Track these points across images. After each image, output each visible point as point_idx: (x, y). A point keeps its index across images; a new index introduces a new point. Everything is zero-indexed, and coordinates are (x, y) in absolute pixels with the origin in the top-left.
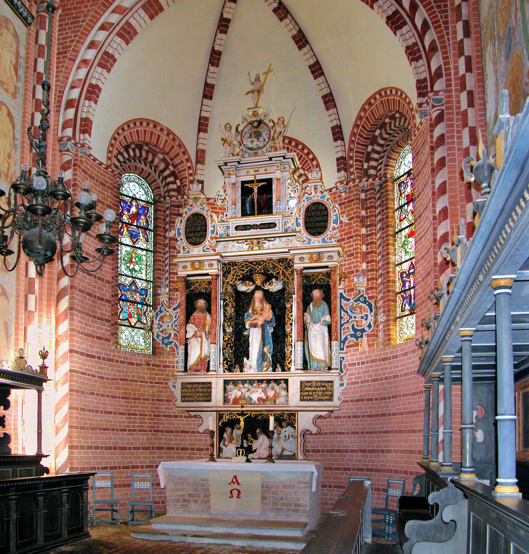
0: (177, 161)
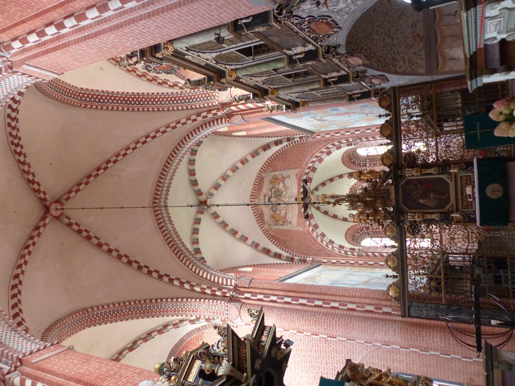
0: (357, 229)
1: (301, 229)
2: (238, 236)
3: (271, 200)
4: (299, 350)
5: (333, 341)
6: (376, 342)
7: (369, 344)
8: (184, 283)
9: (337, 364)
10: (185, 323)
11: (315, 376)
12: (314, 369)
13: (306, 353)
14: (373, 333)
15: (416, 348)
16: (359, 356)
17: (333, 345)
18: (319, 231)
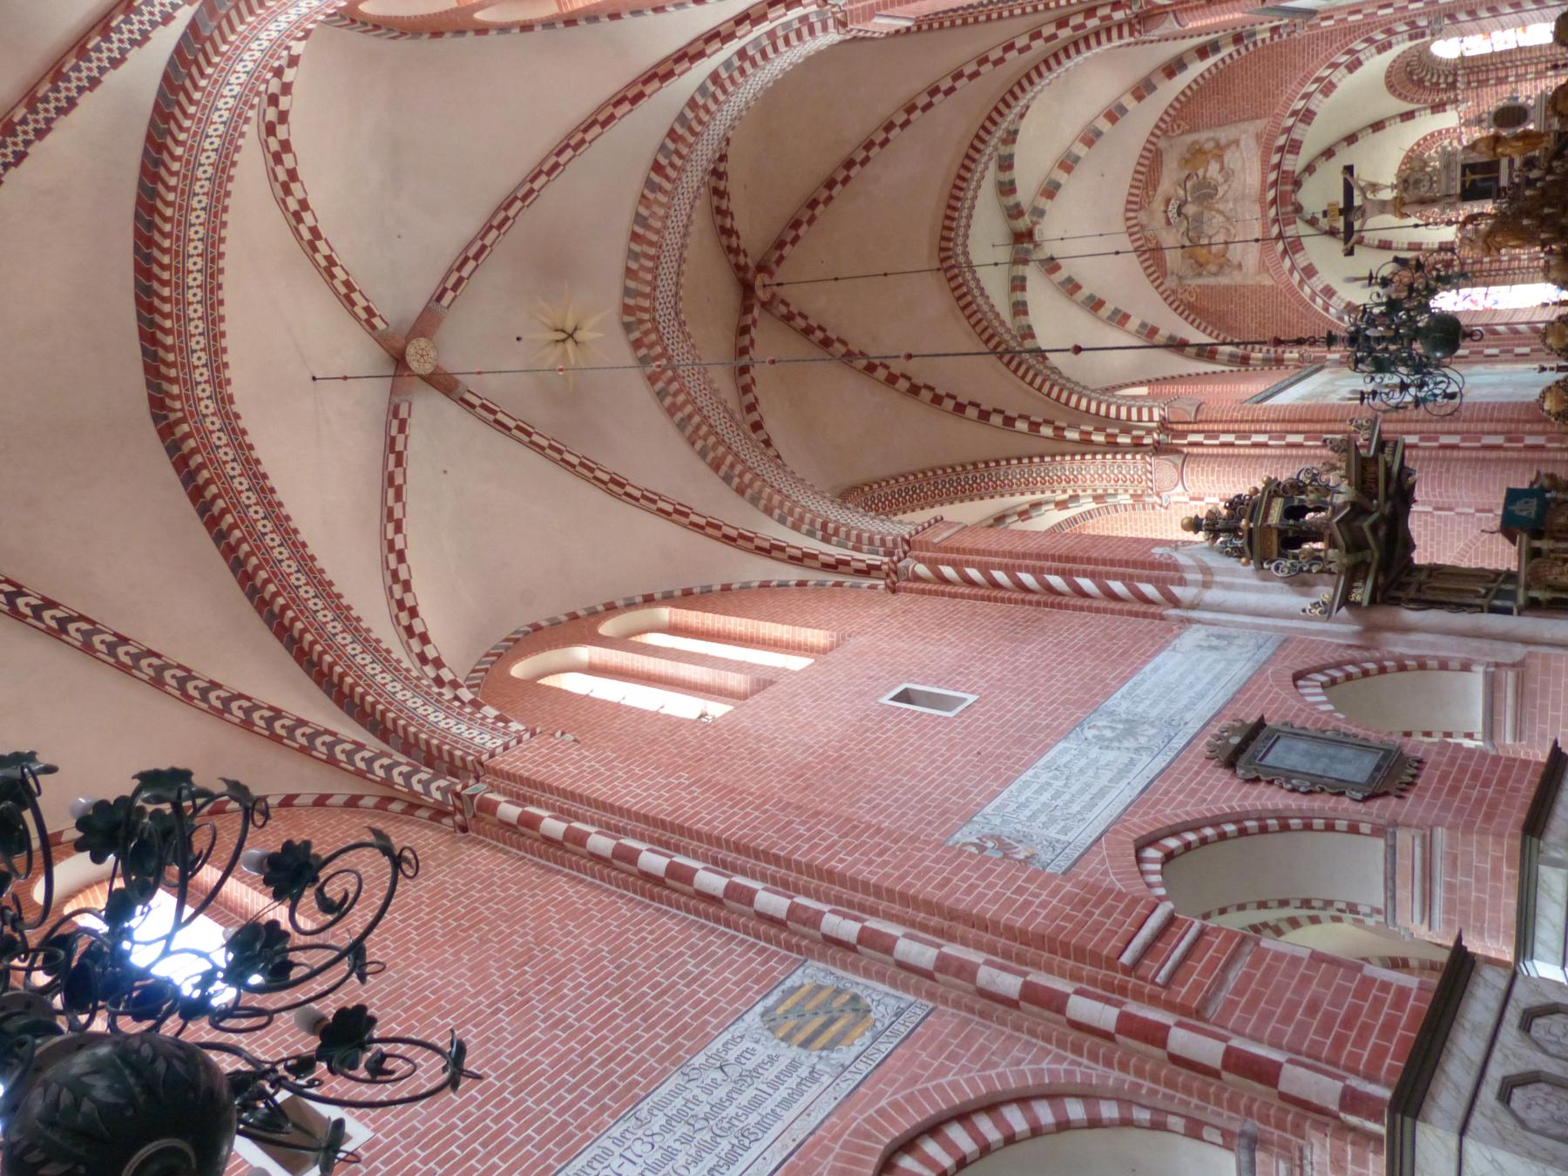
1: (1267, 281)
2: (1105, 312)
3: (1184, 210)
8: (1039, 425)
10: (1044, 508)
18: (1317, 283)
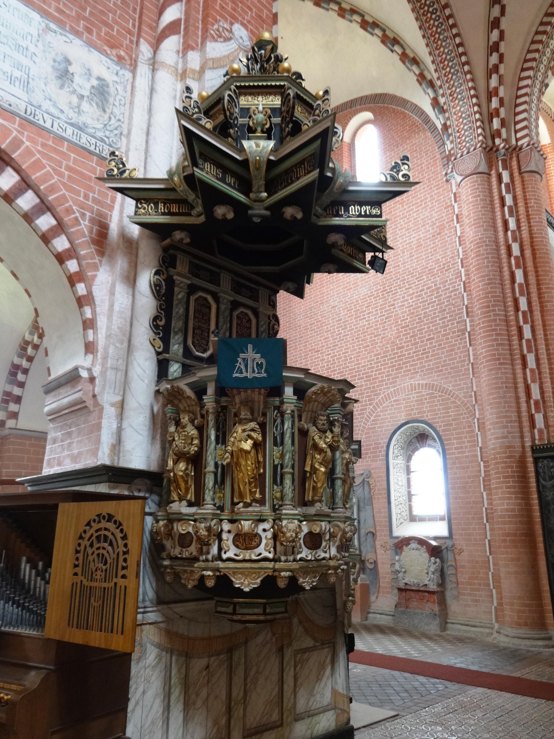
4: (438, 293)
5: (466, 342)
6: (479, 410)
7: (474, 399)
8: (497, 51)
9: (432, 356)
11: (408, 326)
12: (417, 323)
13: (437, 305)
14: (491, 404)
15: (485, 471)
16: (453, 386)
17: (459, 344)
